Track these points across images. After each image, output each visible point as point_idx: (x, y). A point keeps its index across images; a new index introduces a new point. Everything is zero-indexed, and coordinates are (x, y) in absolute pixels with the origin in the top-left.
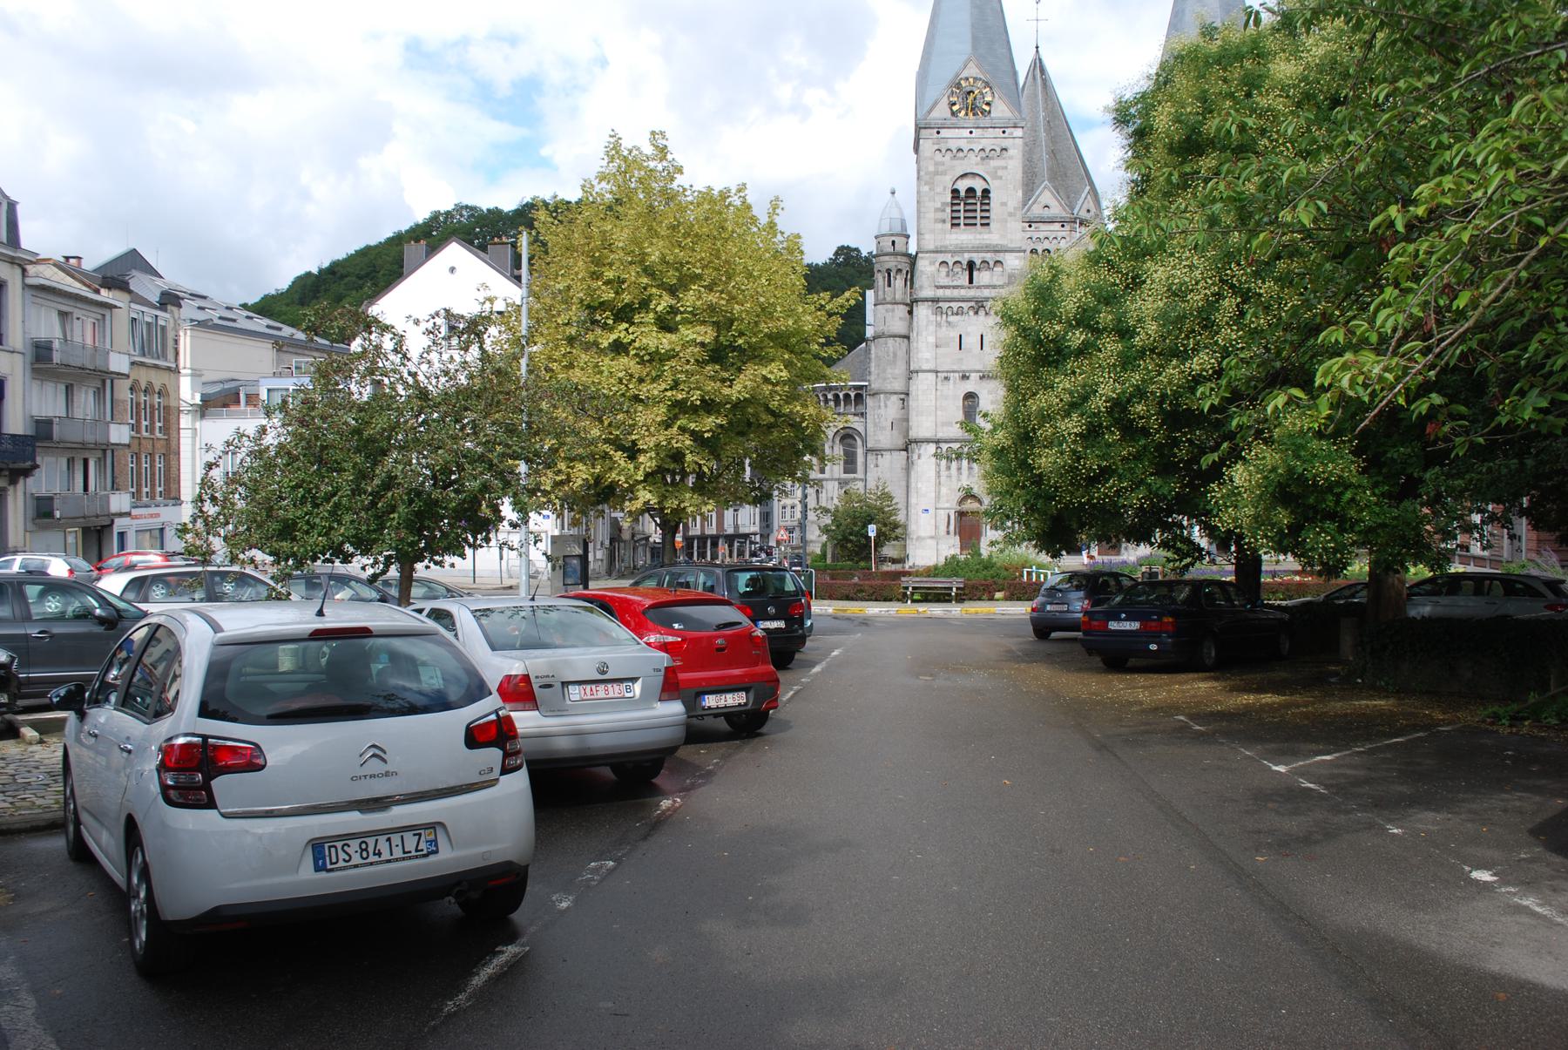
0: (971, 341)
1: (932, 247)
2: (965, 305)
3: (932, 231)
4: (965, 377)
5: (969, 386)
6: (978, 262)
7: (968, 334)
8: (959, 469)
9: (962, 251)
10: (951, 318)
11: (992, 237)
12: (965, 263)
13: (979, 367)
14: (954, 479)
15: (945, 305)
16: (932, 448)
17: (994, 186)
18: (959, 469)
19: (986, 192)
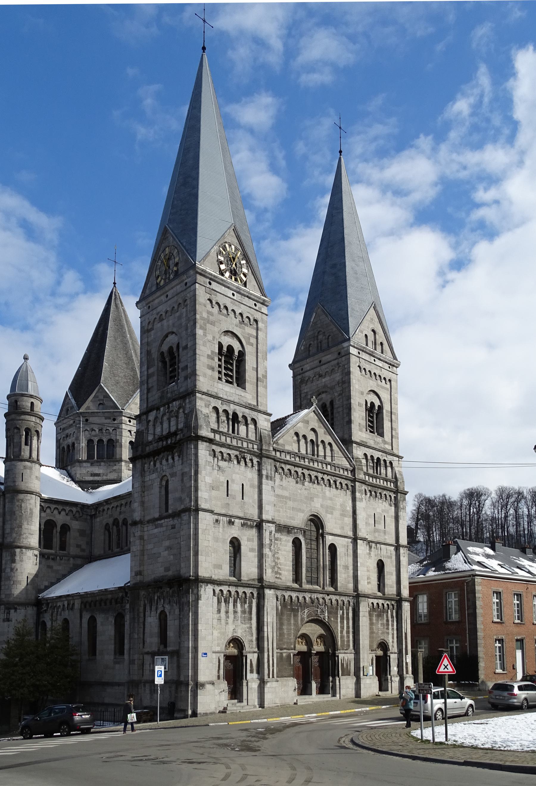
0: (235, 488)
1: (205, 391)
2: (233, 453)
3: (205, 375)
4: (231, 523)
5: (235, 531)
6: (240, 415)
7: (233, 481)
8: (227, 612)
9: (229, 402)
10: (222, 464)
11: (247, 396)
12: (231, 413)
13: (241, 515)
14: (223, 622)
15: (218, 449)
16: (209, 588)
17: (250, 351)
18: (227, 612)
19: (242, 354)
